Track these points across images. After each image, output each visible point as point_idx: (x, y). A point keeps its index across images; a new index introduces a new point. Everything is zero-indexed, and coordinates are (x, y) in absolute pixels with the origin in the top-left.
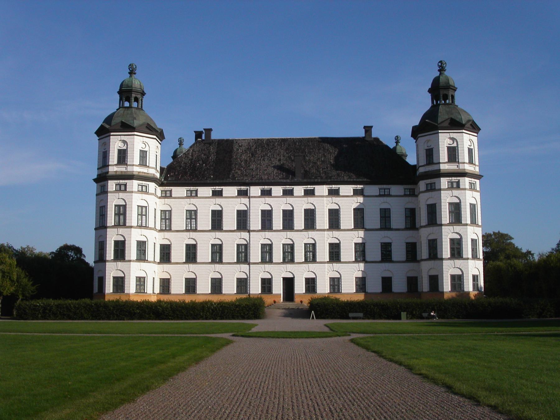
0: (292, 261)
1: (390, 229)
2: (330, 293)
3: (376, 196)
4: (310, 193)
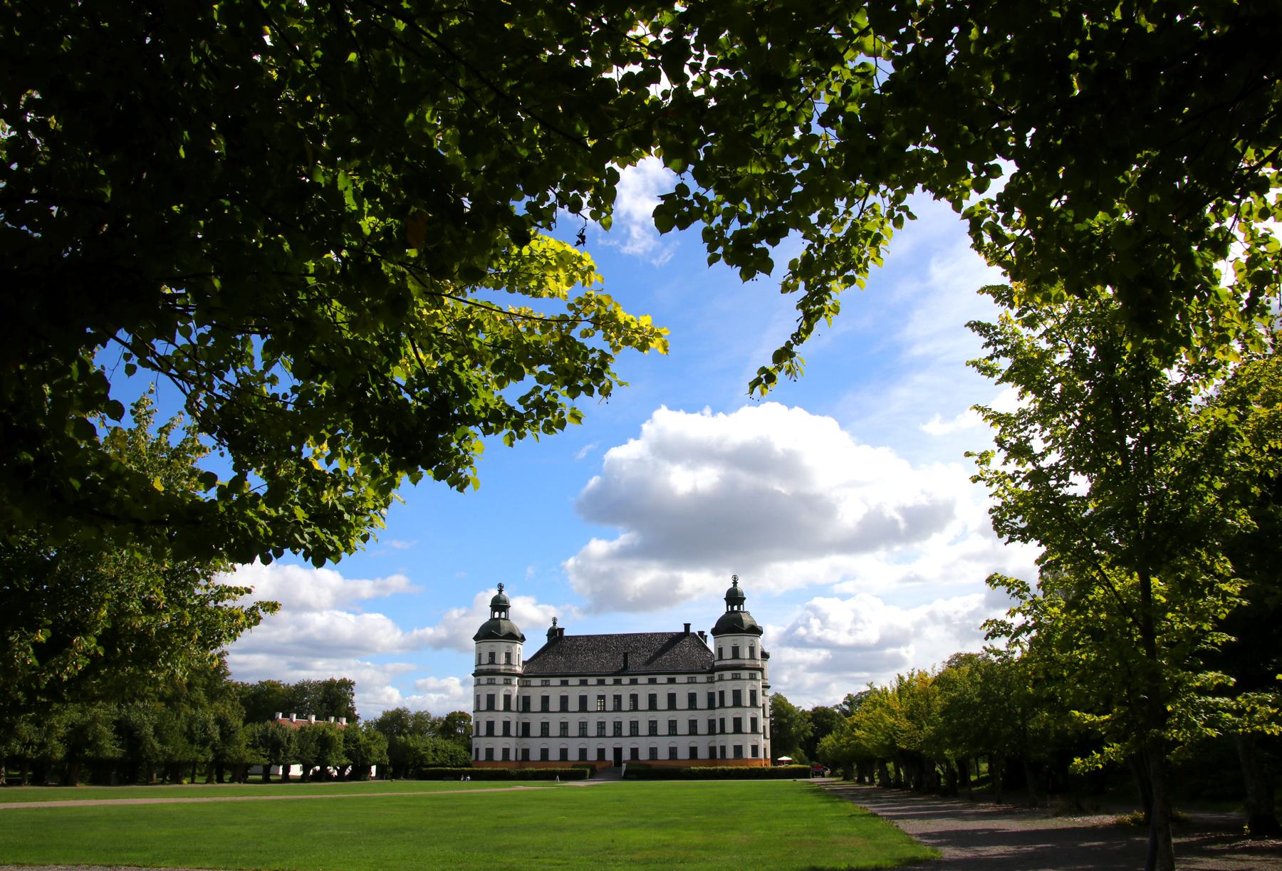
0: (620, 735)
1: (696, 709)
4: (634, 682)
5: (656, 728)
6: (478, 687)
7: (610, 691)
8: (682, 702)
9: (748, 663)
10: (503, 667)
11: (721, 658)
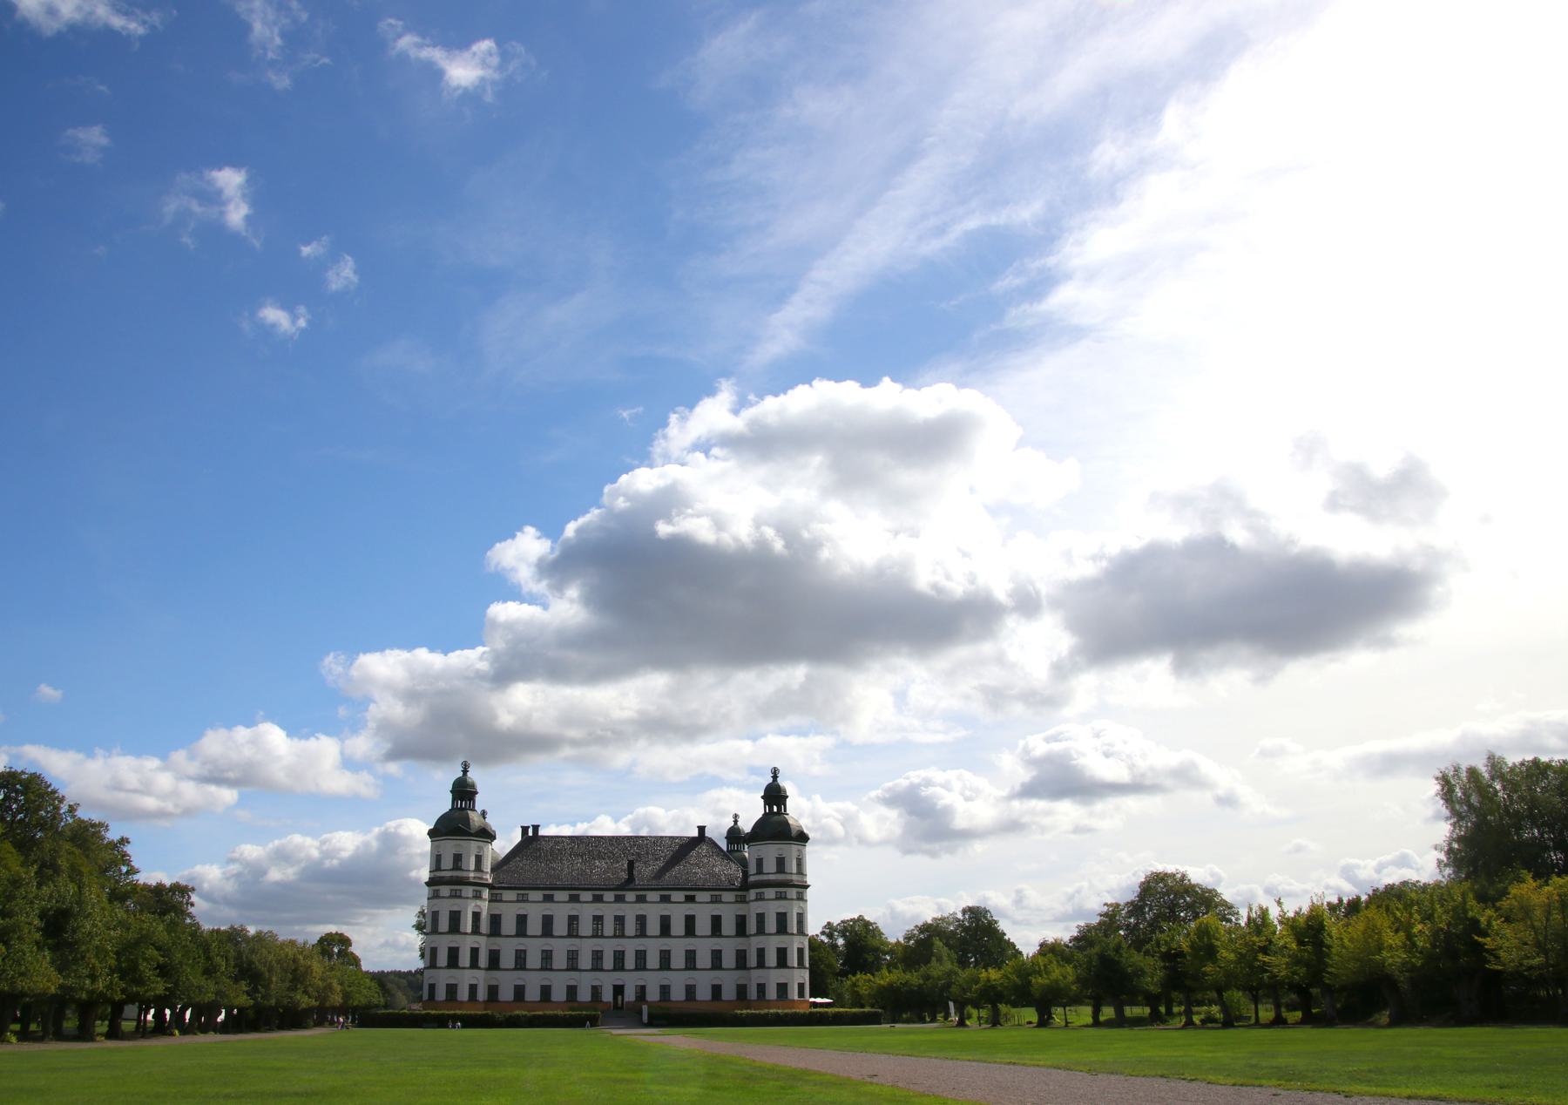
1: (720, 936)
2: (660, 1001)
3: (707, 903)
4: (641, 899)
5: (720, 959)
6: (436, 901)
7: (609, 911)
8: (703, 926)
9: (794, 877)
10: (472, 875)
11: (760, 871)
